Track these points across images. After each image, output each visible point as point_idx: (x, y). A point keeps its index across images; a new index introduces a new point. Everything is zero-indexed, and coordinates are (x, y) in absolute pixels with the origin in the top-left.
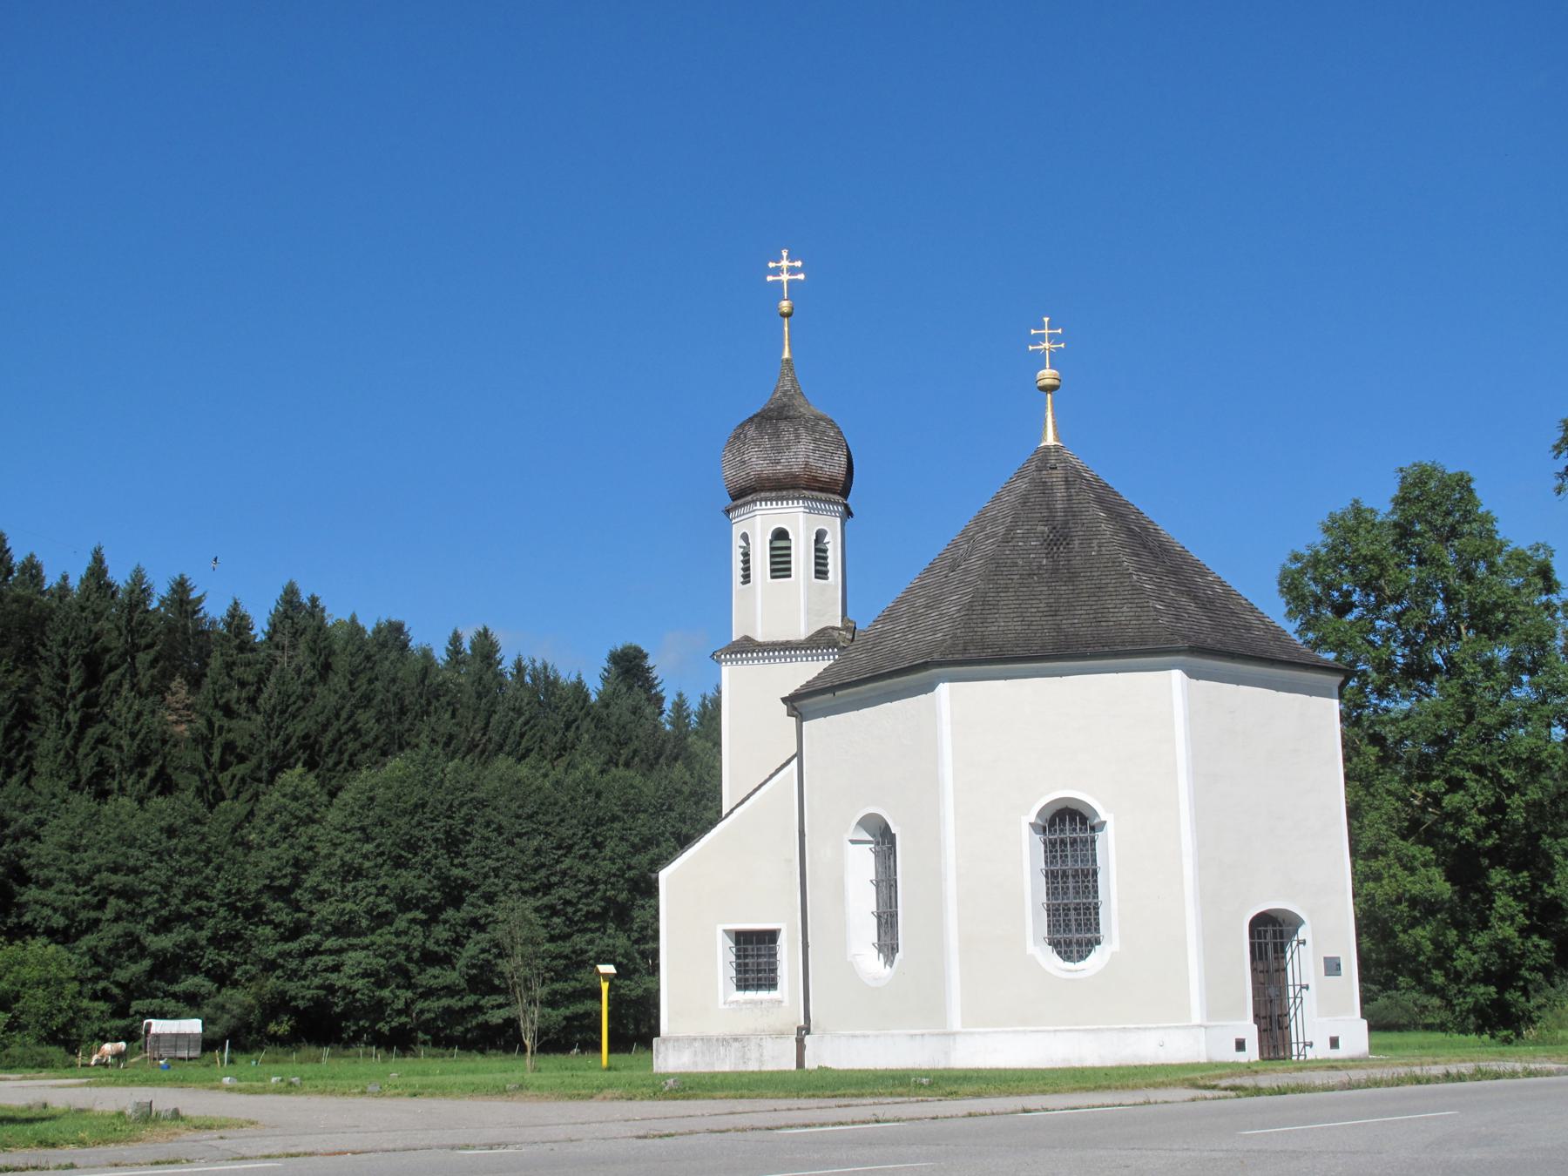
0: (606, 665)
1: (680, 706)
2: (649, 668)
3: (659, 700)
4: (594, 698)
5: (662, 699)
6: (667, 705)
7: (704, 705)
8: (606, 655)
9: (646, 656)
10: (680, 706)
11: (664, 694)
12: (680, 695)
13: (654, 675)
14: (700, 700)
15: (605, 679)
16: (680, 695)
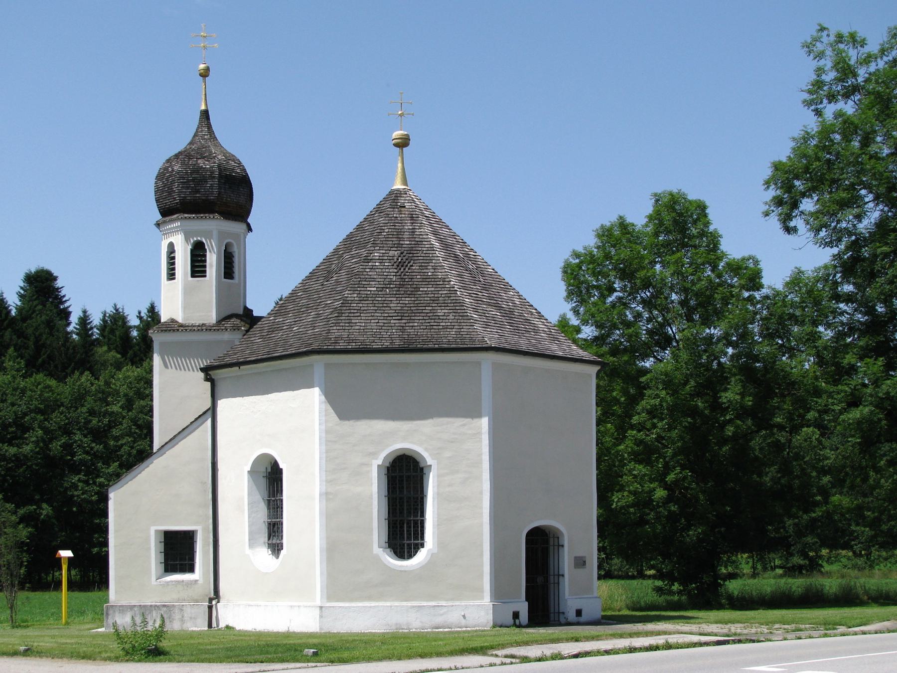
0: (22, 284)
1: (84, 321)
2: (58, 288)
3: (66, 314)
4: (13, 312)
5: (70, 313)
6: (74, 319)
7: (104, 320)
8: (22, 276)
9: (55, 279)
10: (84, 321)
11: (70, 309)
12: (85, 312)
13: (62, 294)
14: (101, 316)
15: (21, 296)
16: (85, 312)
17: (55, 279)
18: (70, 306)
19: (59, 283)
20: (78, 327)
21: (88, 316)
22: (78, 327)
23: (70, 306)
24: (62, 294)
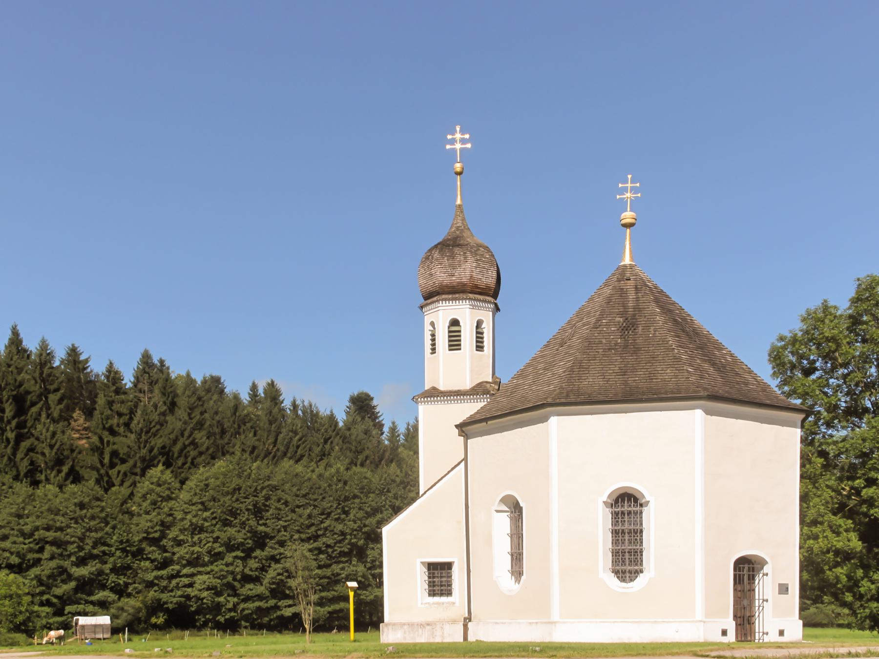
0: (348, 404)
1: (393, 430)
2: (374, 406)
3: (380, 426)
4: (341, 424)
5: (383, 425)
6: (386, 429)
7: (408, 429)
8: (348, 398)
9: (372, 399)
10: (393, 430)
11: (383, 422)
12: (393, 423)
13: (377, 411)
14: (406, 426)
15: (347, 413)
16: (393, 423)
17: (372, 399)
18: (383, 420)
19: (375, 403)
20: (389, 435)
21: (396, 426)
22: (389, 435)
23: (383, 420)
24: (377, 411)
